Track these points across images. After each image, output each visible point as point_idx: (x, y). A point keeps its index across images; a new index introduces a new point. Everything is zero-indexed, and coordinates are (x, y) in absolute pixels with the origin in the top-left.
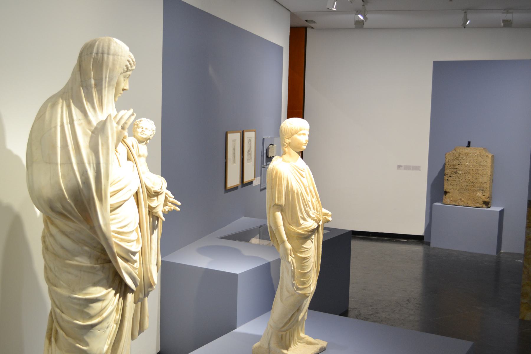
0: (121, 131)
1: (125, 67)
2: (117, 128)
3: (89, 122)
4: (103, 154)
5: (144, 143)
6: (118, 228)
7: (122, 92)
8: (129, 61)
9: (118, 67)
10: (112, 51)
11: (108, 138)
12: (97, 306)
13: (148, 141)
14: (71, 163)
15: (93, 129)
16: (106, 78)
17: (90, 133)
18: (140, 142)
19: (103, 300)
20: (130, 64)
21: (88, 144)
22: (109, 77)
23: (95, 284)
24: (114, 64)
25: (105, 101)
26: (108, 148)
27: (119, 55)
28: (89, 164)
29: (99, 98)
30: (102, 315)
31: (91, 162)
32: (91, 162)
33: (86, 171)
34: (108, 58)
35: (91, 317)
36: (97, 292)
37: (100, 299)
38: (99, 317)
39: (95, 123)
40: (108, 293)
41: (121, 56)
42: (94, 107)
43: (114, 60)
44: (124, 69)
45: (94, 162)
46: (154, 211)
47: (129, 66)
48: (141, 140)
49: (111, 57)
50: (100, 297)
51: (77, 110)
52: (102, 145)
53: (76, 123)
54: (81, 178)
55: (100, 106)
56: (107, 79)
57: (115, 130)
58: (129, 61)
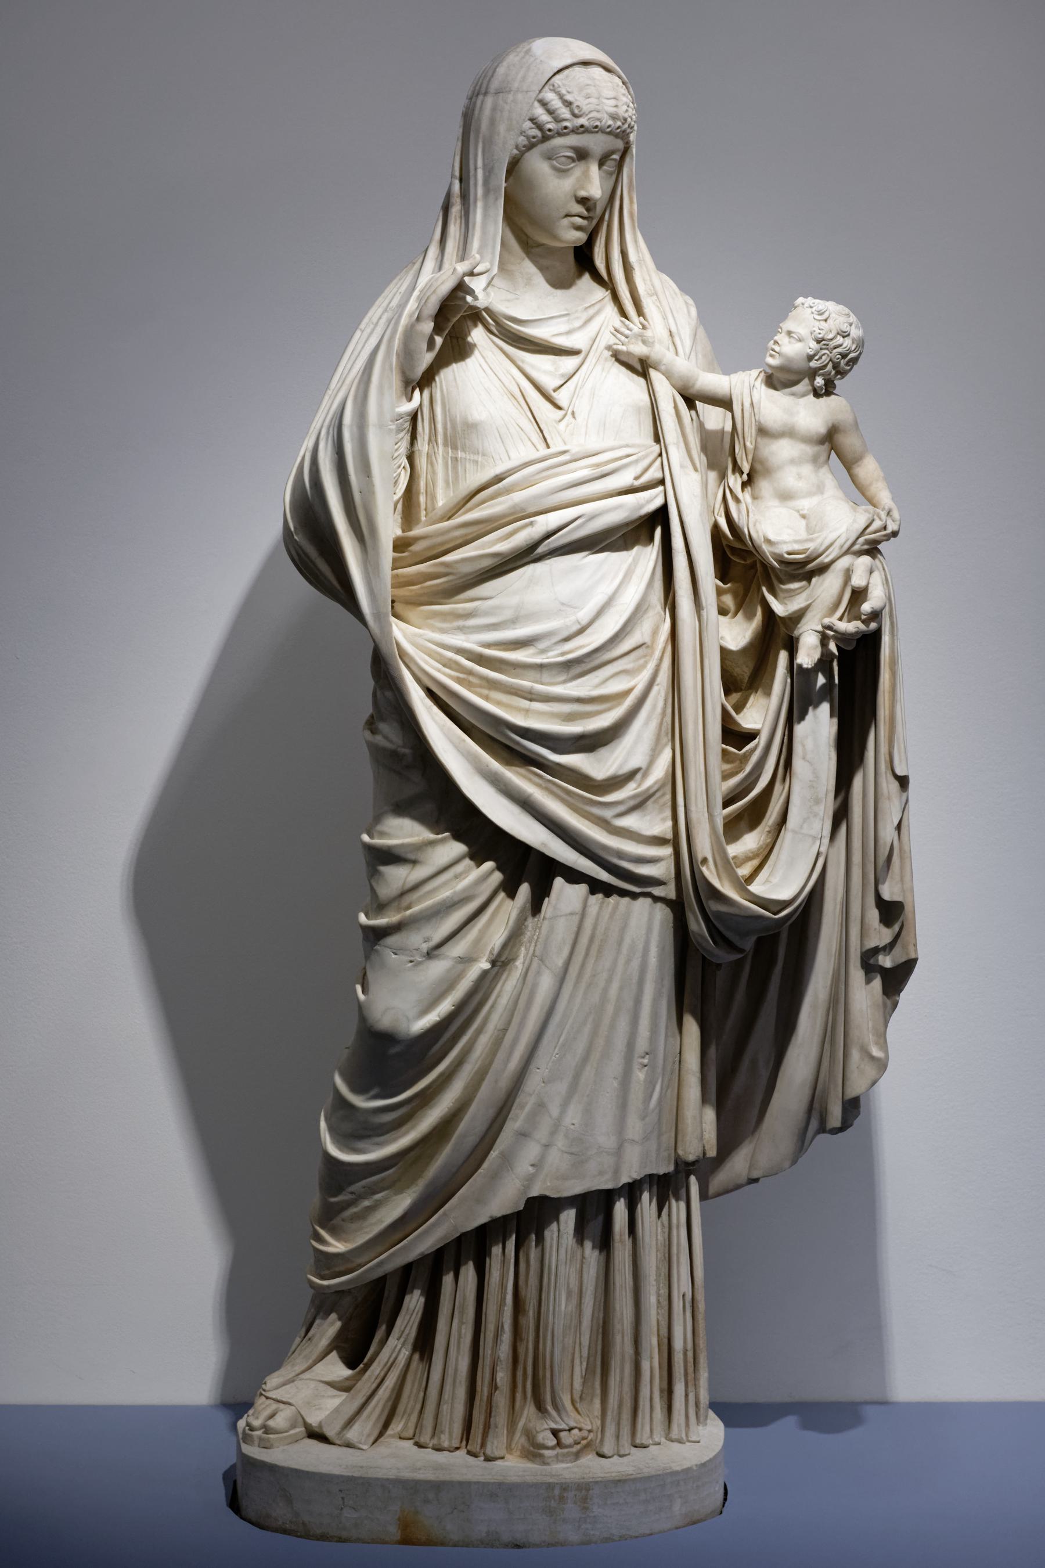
1: (529, 124)
6: (489, 645)
8: (544, 104)
9: (502, 128)
10: (494, 85)
12: (397, 876)
16: (476, 169)
19: (414, 862)
20: (550, 112)
22: (484, 165)
23: (401, 809)
24: (493, 122)
25: (475, 244)
27: (510, 91)
30: (409, 907)
34: (483, 102)
35: (380, 907)
36: (403, 831)
37: (402, 853)
38: (399, 910)
40: (432, 843)
41: (518, 90)
43: (494, 109)
44: (522, 133)
46: (796, 633)
47: (544, 117)
49: (489, 101)
50: (402, 845)
56: (480, 173)
58: (544, 104)
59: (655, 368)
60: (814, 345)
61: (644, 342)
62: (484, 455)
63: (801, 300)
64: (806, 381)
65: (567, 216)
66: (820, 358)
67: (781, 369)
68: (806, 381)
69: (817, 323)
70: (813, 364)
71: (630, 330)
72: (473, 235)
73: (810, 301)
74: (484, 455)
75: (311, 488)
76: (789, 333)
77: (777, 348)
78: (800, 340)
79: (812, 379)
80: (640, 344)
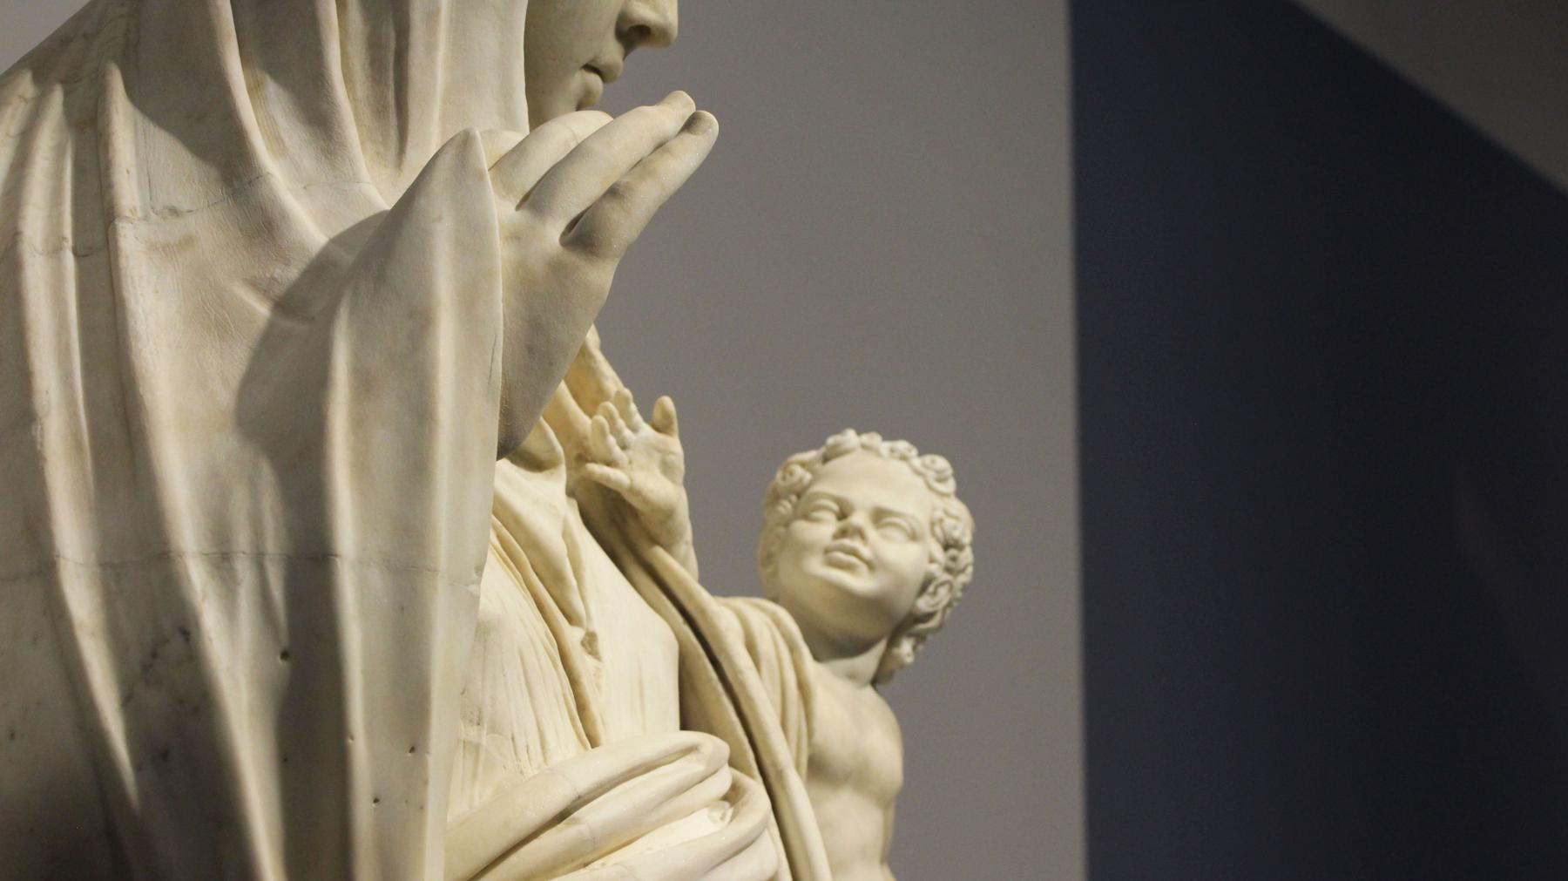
0: (557, 269)
2: (516, 237)
3: (260, 224)
4: (361, 468)
5: (868, 662)
7: (612, 52)
11: (421, 321)
13: (906, 648)
14: (45, 569)
15: (292, 273)
17: (262, 310)
18: (831, 644)
21: (226, 397)
26: (420, 413)
28: (221, 560)
29: (374, 44)
31: (242, 541)
32: (242, 541)
33: (187, 631)
39: (312, 224)
42: (316, 115)
45: (273, 545)
48: (837, 621)
51: (165, 145)
52: (364, 383)
53: (132, 240)
54: (128, 701)
55: (379, 112)
57: (502, 253)
59: (668, 548)
60: (939, 554)
61: (666, 468)
62: (494, 729)
63: (850, 437)
64: (880, 648)
65: (591, 68)
66: (935, 593)
67: (873, 605)
68: (880, 648)
69: (938, 502)
70: (924, 604)
71: (634, 429)
72: (431, 47)
73: (874, 439)
74: (494, 729)
75: (138, 767)
76: (880, 516)
77: (866, 552)
78: (914, 537)
79: (893, 641)
80: (657, 472)
